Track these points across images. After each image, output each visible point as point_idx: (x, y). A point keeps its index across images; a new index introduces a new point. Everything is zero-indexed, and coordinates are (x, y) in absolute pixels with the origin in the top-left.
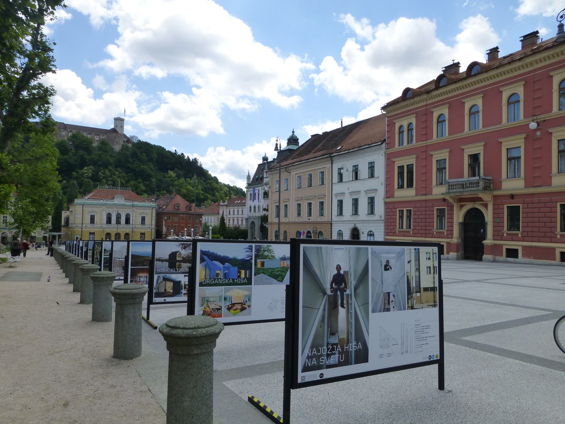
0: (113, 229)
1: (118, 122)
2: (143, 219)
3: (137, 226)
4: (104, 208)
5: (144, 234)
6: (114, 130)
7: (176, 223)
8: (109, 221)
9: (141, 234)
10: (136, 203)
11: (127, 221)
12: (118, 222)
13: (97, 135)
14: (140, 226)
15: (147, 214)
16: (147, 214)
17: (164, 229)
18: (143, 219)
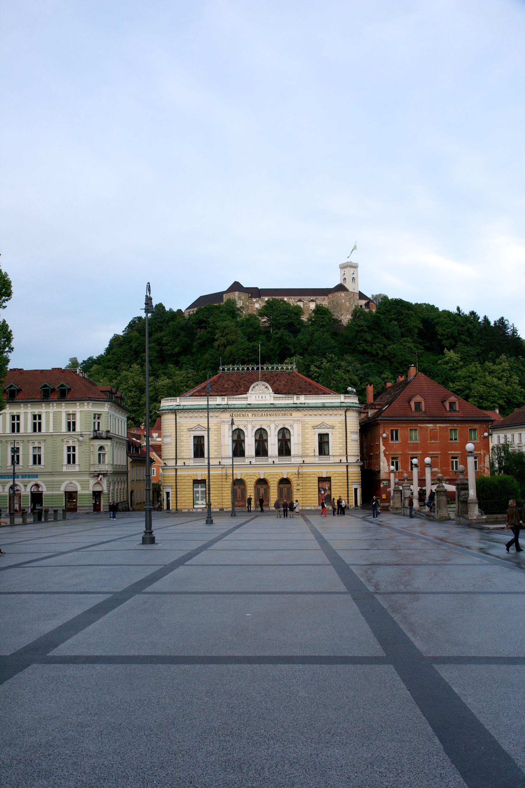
0: (250, 469)
1: (347, 270)
2: (323, 442)
3: (307, 460)
4: (226, 416)
5: (328, 479)
6: (341, 288)
7: (415, 447)
8: (238, 451)
9: (321, 480)
10: (302, 399)
11: (285, 450)
12: (261, 450)
13: (312, 301)
14: (317, 460)
15: (333, 427)
16: (333, 427)
17: (385, 466)
18: (323, 442)
